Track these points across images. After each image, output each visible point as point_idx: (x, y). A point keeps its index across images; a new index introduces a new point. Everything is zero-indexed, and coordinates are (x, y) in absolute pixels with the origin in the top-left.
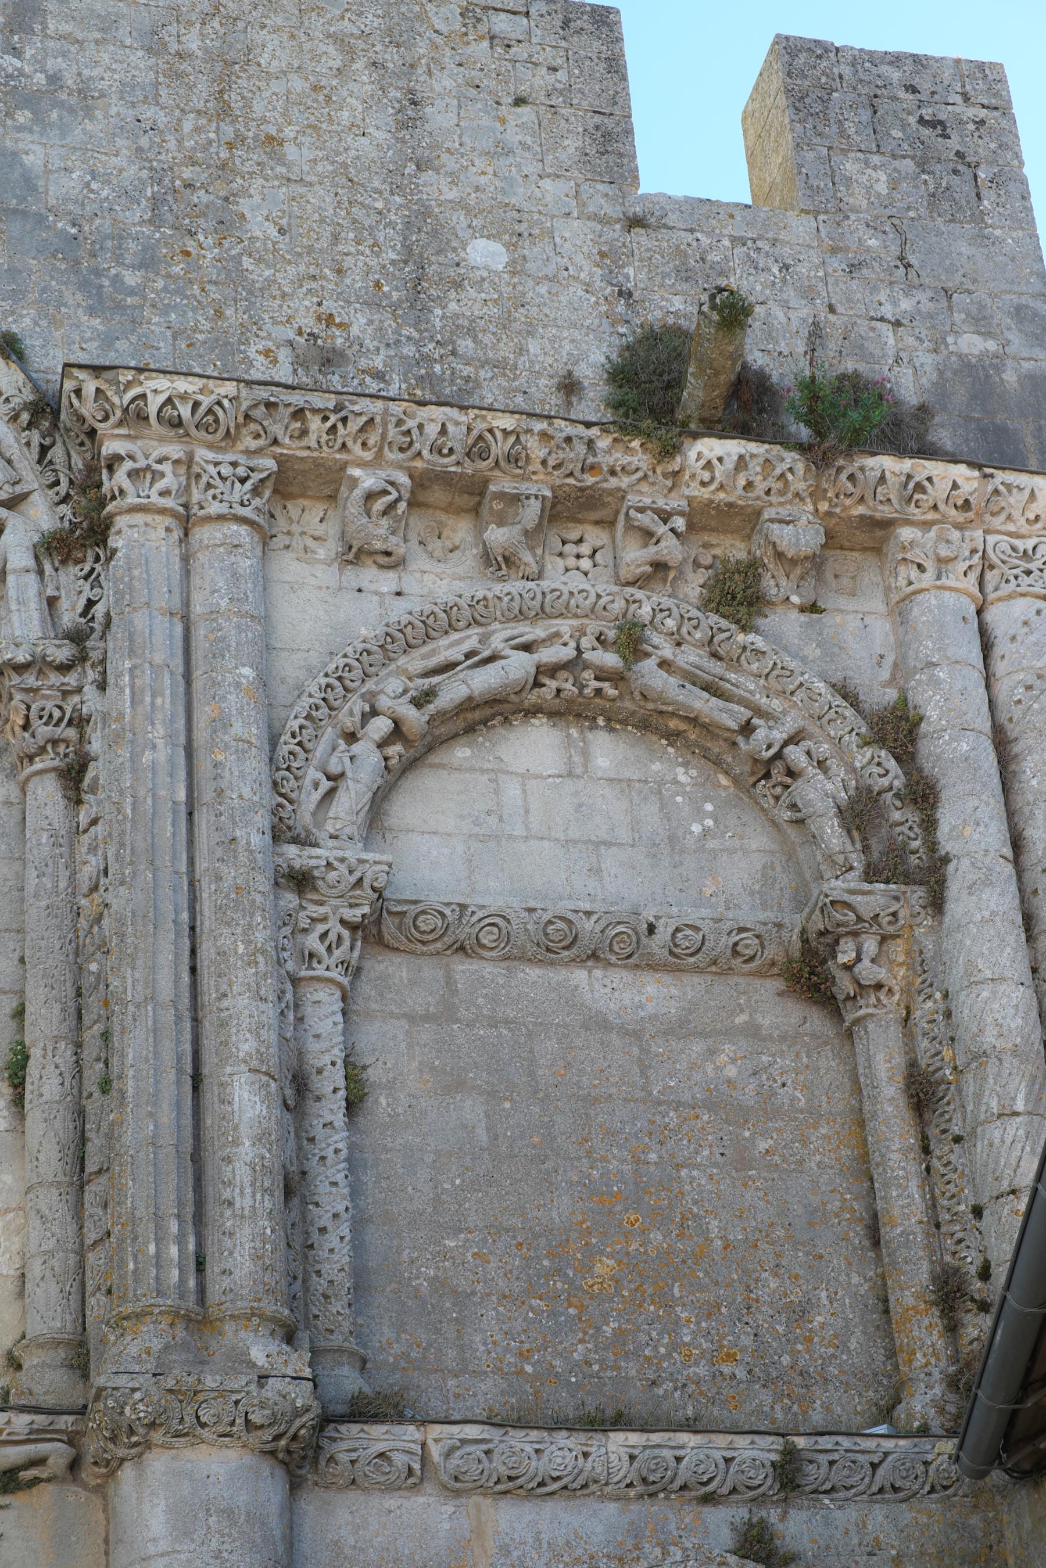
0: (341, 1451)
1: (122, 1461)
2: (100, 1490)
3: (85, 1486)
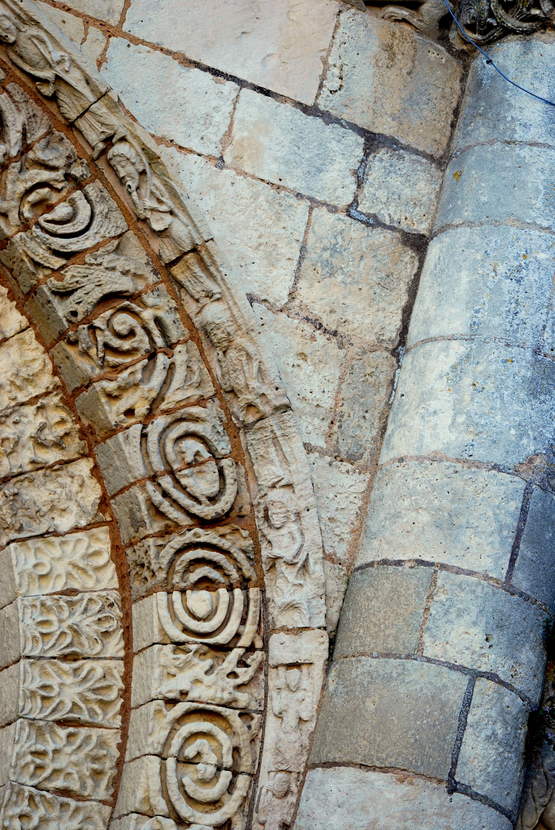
1: (507, 32)
3: (450, 49)
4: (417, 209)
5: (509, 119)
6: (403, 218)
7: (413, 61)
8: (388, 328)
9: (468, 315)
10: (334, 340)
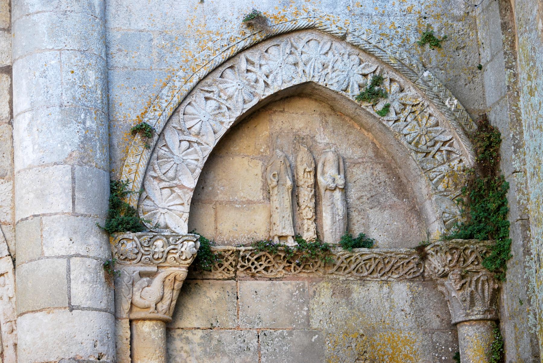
4: (3, 55)
5: (26, 4)
8: (4, 113)
9: (29, 99)
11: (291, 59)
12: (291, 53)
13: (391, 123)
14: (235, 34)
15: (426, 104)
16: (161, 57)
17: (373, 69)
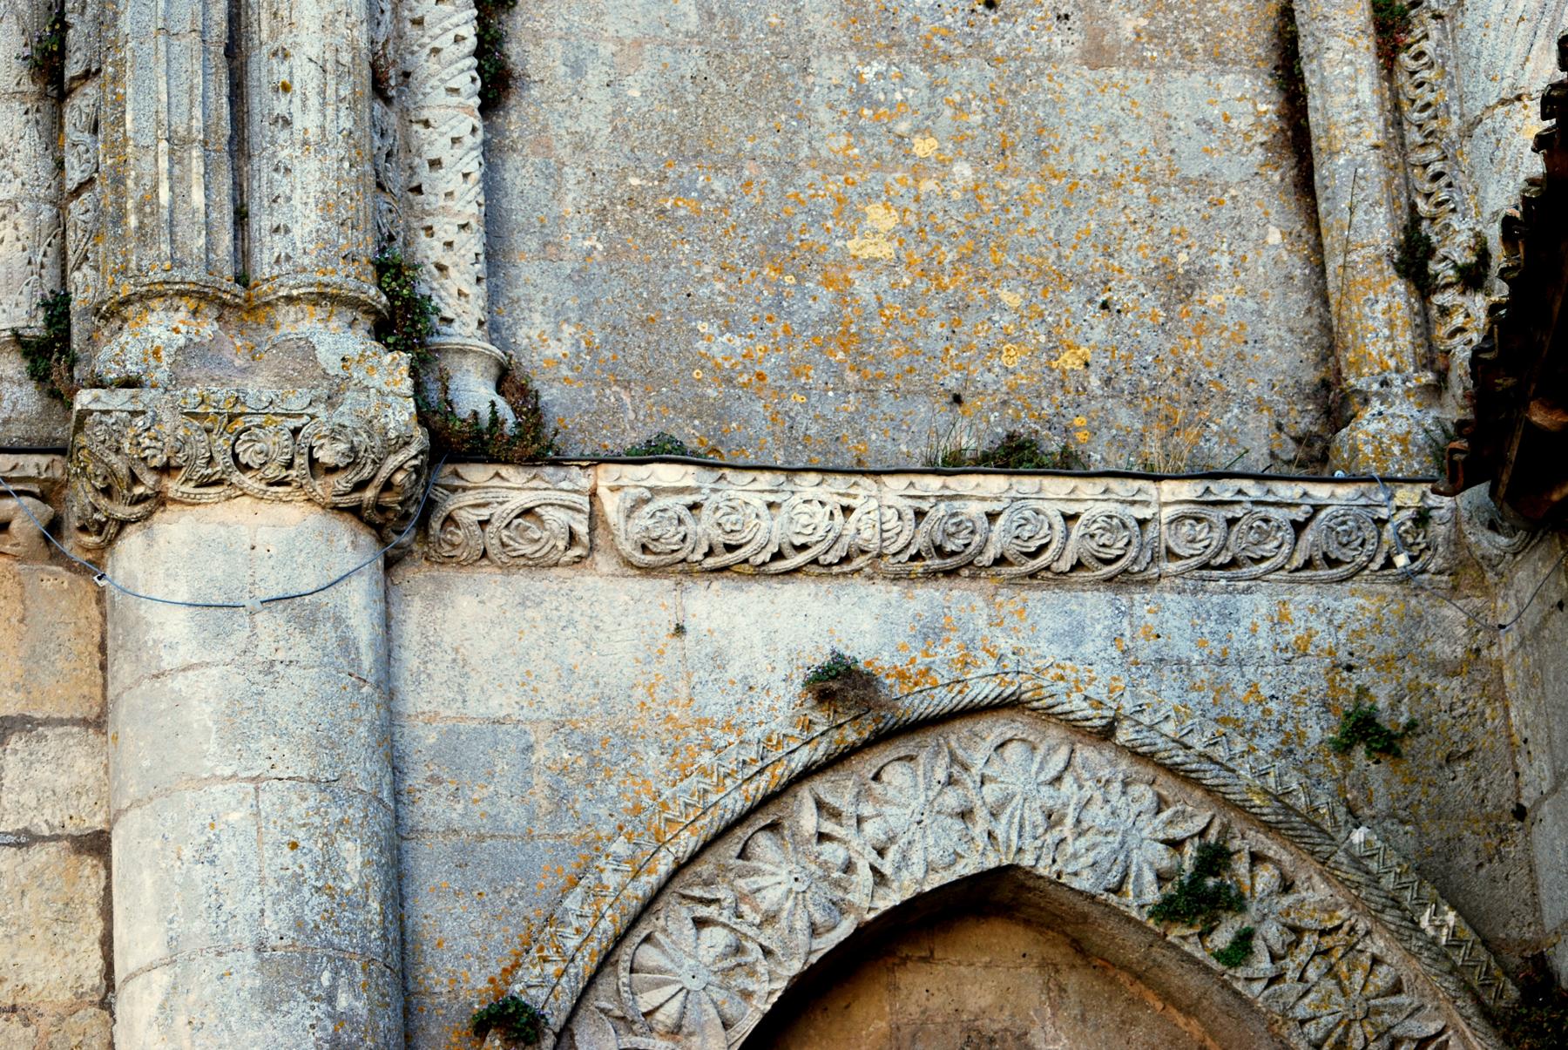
0: (463, 507)
1: (123, 524)
2: (93, 567)
3: (70, 565)
4: (84, 798)
5: (150, 643)
6: (66, 818)
7: (23, 602)
10: (15, 1018)
11: (952, 799)
12: (951, 781)
13: (1258, 987)
14: (780, 724)
15: (1361, 927)
16: (560, 800)
17: (1199, 823)
